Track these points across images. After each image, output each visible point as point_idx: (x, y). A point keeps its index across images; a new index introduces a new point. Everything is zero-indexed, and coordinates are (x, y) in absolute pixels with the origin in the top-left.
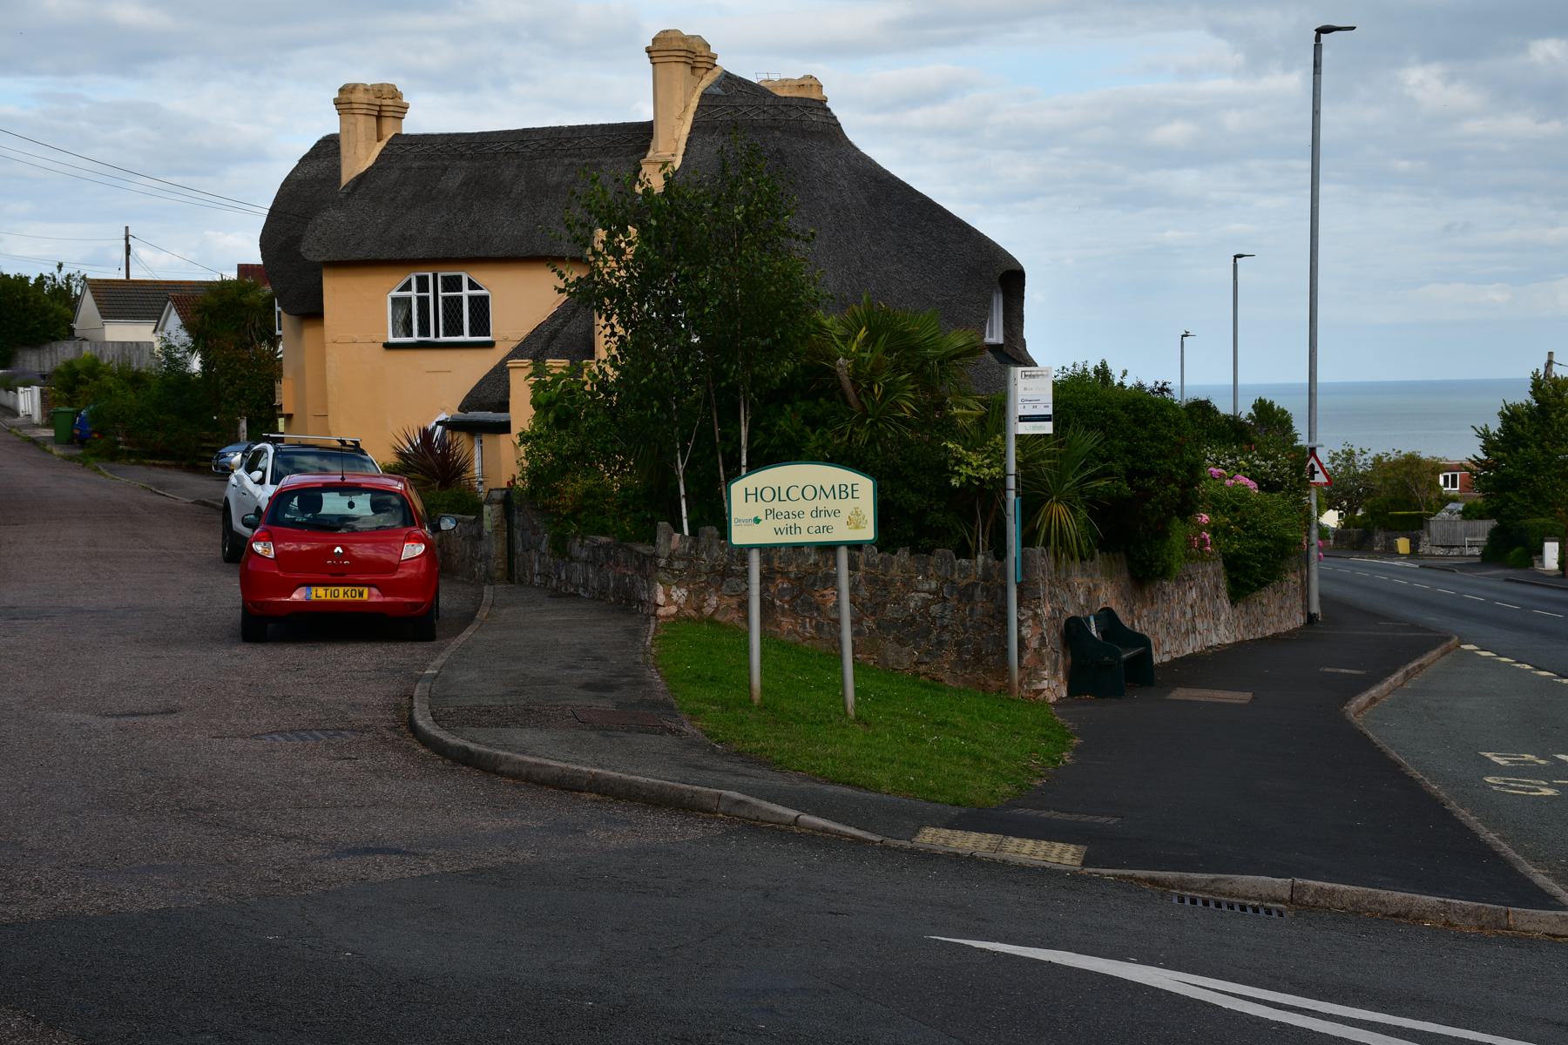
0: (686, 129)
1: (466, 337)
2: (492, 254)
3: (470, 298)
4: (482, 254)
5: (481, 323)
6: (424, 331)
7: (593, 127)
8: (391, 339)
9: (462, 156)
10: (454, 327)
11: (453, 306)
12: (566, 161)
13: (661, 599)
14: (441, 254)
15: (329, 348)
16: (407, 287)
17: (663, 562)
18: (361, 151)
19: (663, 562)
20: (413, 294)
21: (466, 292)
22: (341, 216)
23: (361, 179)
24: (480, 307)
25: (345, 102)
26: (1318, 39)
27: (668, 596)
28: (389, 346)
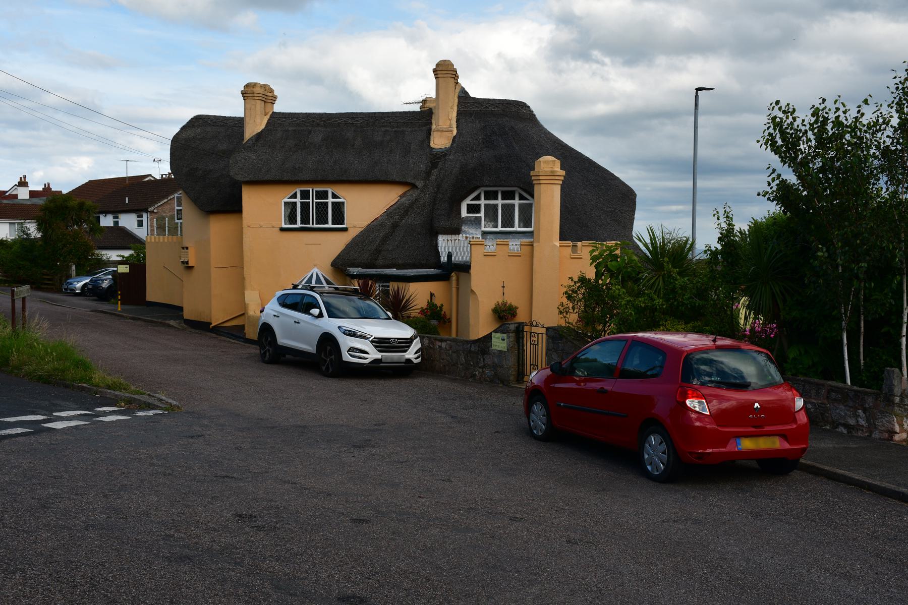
0: (455, 114)
1: (330, 225)
2: (351, 179)
3: (333, 203)
4: (344, 178)
5: (339, 217)
6: (305, 220)
7: (409, 112)
8: (284, 226)
9: (318, 125)
10: (322, 219)
11: (322, 208)
12: (383, 129)
13: (897, 428)
14: (320, 178)
15: (245, 230)
16: (294, 196)
17: (897, 399)
18: (258, 120)
19: (897, 399)
20: (298, 200)
21: (330, 200)
22: (252, 155)
23: (259, 136)
24: (339, 209)
25: (249, 92)
26: (697, 93)
27: (901, 425)
28: (282, 230)
